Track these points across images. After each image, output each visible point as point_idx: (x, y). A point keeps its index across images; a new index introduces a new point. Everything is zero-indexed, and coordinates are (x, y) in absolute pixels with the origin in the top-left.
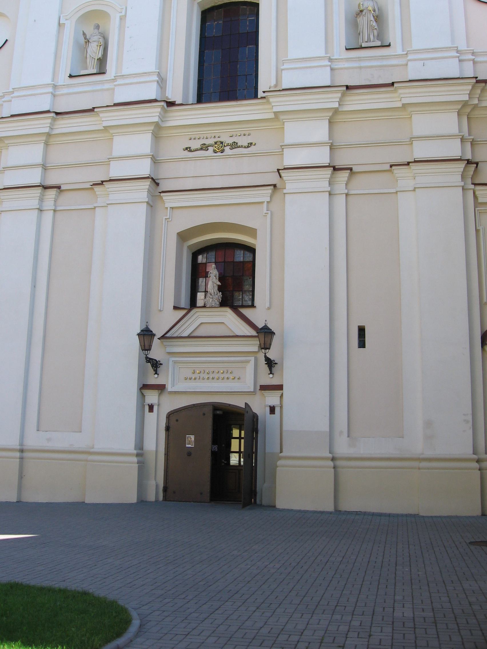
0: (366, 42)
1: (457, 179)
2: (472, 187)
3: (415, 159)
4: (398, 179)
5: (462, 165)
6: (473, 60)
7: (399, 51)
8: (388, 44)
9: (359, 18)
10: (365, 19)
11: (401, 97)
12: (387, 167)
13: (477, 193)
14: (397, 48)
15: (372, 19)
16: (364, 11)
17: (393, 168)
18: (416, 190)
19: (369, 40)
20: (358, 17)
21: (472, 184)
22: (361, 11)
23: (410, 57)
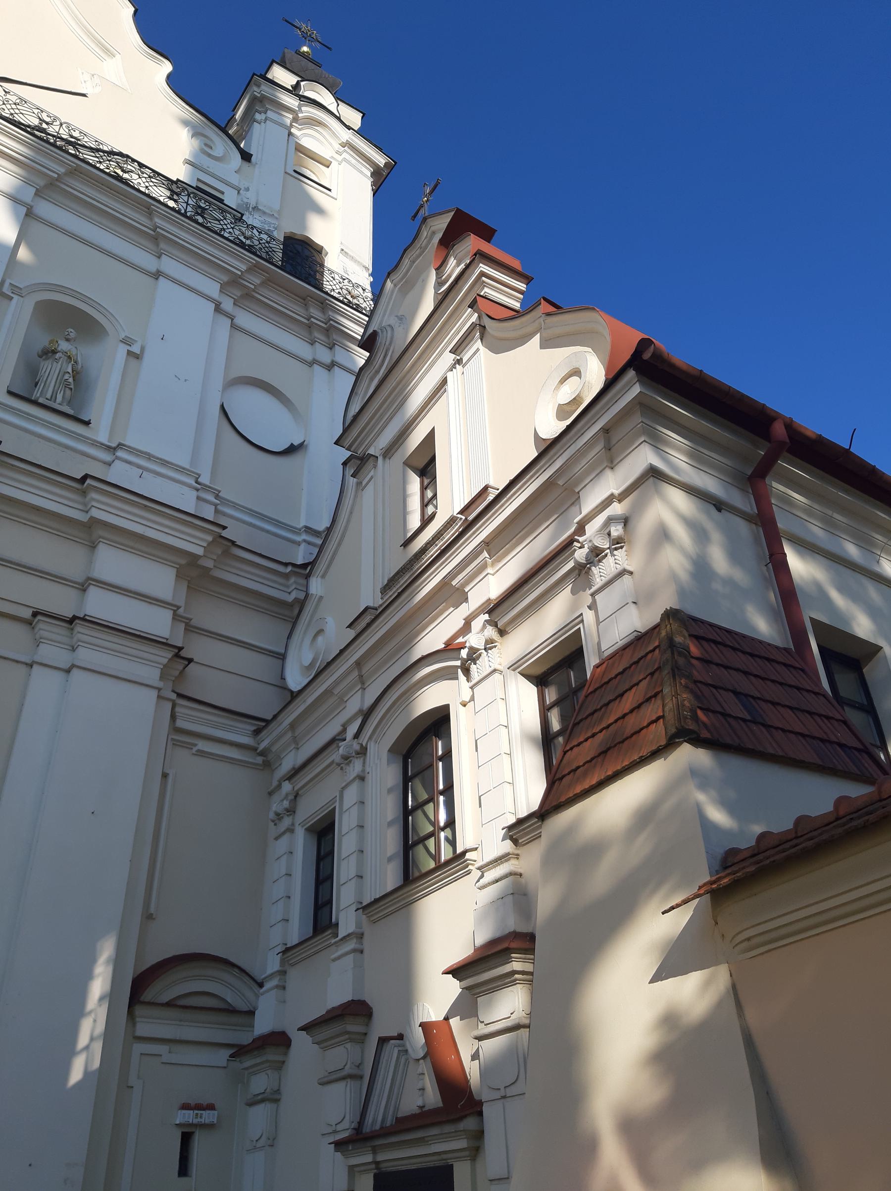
0: (47, 399)
1: (152, 675)
2: (174, 696)
3: (85, 615)
4: (42, 640)
5: (165, 656)
6: (216, 505)
7: (103, 438)
8: (87, 420)
9: (44, 360)
10: (57, 367)
11: (93, 506)
12: (27, 614)
13: (177, 709)
14: (101, 432)
15: (70, 370)
16: (58, 353)
17: (39, 617)
18: (75, 671)
19: (53, 398)
20: (44, 357)
21: (173, 691)
22: (54, 352)
23: (120, 453)
